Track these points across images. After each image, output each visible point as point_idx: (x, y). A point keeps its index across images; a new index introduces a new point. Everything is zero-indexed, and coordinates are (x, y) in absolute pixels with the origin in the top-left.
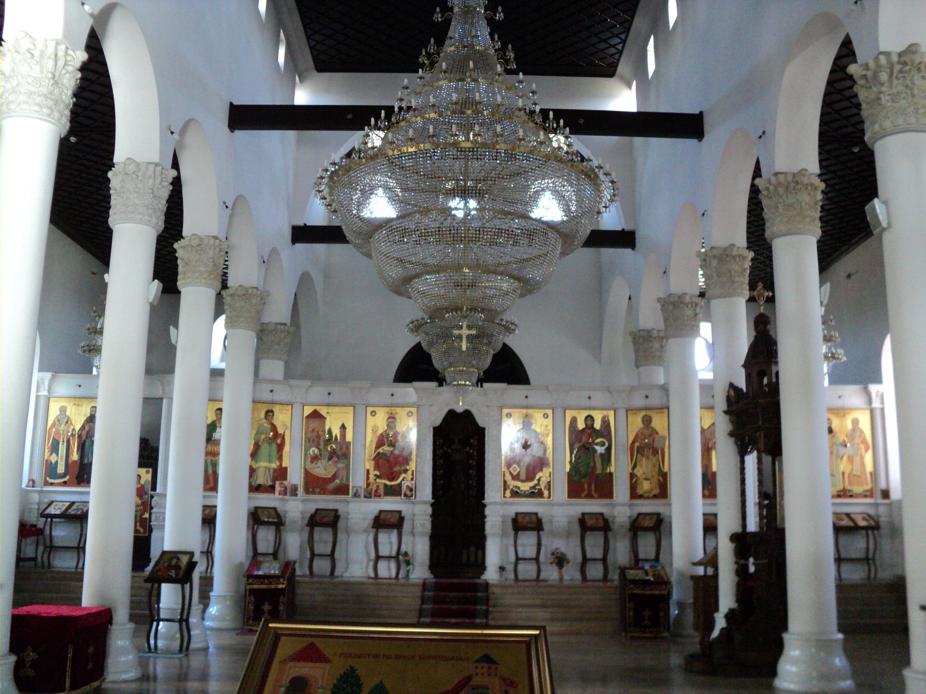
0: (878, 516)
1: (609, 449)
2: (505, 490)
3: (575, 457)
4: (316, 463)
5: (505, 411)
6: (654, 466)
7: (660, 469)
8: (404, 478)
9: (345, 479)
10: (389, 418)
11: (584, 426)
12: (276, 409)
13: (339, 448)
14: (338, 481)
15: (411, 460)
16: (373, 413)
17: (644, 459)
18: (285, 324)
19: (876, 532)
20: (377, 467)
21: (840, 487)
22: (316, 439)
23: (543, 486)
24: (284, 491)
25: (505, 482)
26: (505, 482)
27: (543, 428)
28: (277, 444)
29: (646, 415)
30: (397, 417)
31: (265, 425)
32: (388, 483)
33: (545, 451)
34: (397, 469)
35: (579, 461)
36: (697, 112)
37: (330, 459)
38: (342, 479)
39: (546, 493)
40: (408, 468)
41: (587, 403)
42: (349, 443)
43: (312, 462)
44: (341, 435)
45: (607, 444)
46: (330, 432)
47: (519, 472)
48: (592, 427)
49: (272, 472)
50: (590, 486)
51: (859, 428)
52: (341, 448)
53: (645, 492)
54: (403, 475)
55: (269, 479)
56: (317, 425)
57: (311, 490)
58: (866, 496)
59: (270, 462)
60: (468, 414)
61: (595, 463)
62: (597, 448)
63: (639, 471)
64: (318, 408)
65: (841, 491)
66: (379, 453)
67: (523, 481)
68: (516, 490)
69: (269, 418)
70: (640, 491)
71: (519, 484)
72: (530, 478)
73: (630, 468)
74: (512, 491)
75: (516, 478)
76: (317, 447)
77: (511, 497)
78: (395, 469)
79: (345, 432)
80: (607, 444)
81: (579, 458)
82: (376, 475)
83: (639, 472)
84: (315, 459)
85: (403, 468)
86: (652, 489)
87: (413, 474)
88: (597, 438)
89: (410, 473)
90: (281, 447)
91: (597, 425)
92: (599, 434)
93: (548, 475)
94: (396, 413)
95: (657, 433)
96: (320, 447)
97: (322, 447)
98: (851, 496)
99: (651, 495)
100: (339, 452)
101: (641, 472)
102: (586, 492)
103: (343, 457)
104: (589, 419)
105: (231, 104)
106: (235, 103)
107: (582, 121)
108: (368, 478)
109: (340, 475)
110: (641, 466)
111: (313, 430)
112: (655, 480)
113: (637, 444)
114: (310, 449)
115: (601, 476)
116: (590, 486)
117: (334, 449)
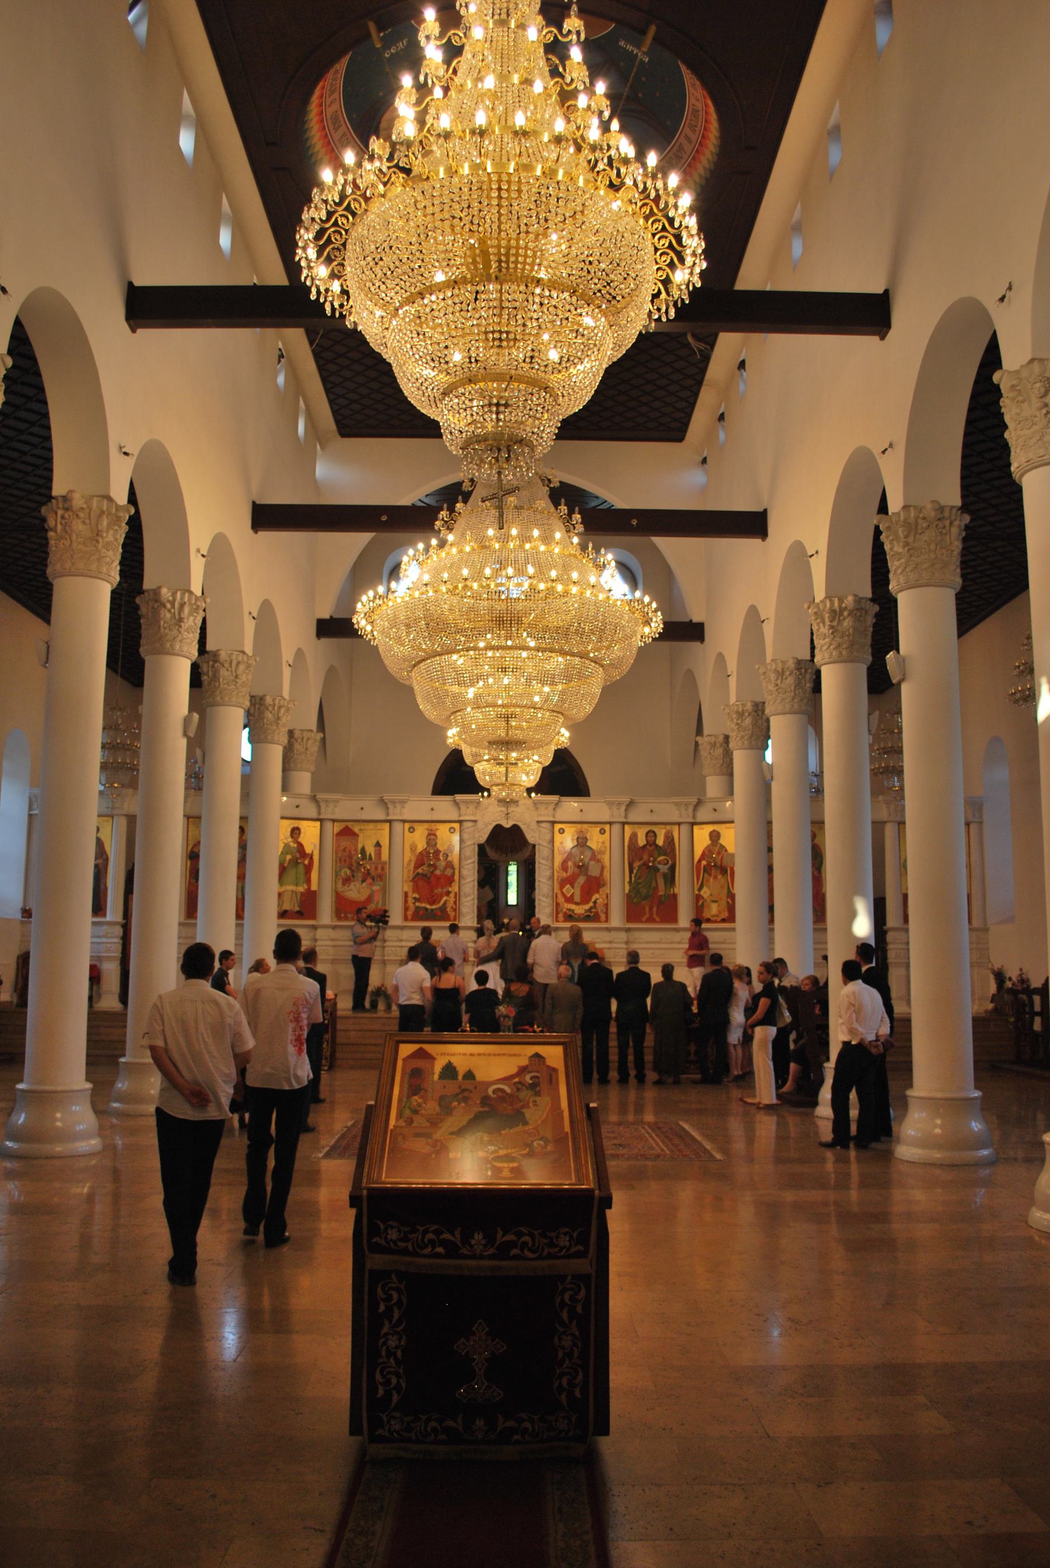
1: (673, 868)
2: (557, 913)
3: (635, 876)
5: (557, 827)
6: (722, 887)
7: (729, 888)
8: (446, 900)
9: (380, 902)
10: (429, 835)
11: (645, 843)
12: (304, 825)
13: (373, 869)
15: (454, 881)
16: (412, 830)
17: (711, 879)
18: (311, 731)
20: (416, 889)
23: (600, 908)
25: (558, 904)
26: (558, 904)
27: (600, 844)
28: (305, 865)
29: (714, 831)
30: (438, 833)
31: (292, 844)
32: (428, 907)
33: (603, 868)
34: (438, 891)
35: (640, 881)
36: (761, 510)
38: (377, 903)
39: (603, 916)
40: (450, 889)
41: (648, 819)
42: (385, 863)
43: (344, 884)
44: (375, 855)
45: (670, 862)
46: (363, 851)
47: (573, 894)
48: (654, 843)
49: (299, 897)
50: (651, 909)
52: (376, 868)
53: (712, 916)
54: (445, 898)
55: (296, 905)
59: (297, 885)
60: (516, 831)
61: (657, 883)
62: (659, 866)
63: (705, 892)
64: (350, 824)
66: (418, 874)
67: (577, 904)
68: (571, 913)
69: (295, 835)
70: (706, 915)
71: (573, 907)
72: (585, 900)
73: (696, 887)
74: (565, 913)
75: (570, 900)
76: (350, 868)
77: (565, 921)
78: (436, 891)
79: (380, 851)
80: (670, 862)
81: (639, 878)
82: (415, 898)
83: (705, 893)
84: (347, 881)
85: (445, 890)
86: (720, 912)
87: (456, 897)
88: (660, 855)
89: (452, 895)
90: (308, 869)
91: (660, 842)
92: (660, 850)
93: (605, 897)
94: (437, 830)
95: (726, 850)
99: (719, 919)
100: (373, 873)
101: (708, 893)
102: (647, 916)
104: (651, 835)
105: (254, 503)
106: (258, 502)
107: (634, 522)
108: (406, 901)
110: (709, 887)
111: (344, 850)
112: (724, 903)
113: (704, 863)
114: (340, 871)
115: (663, 899)
116: (651, 909)
117: (368, 870)
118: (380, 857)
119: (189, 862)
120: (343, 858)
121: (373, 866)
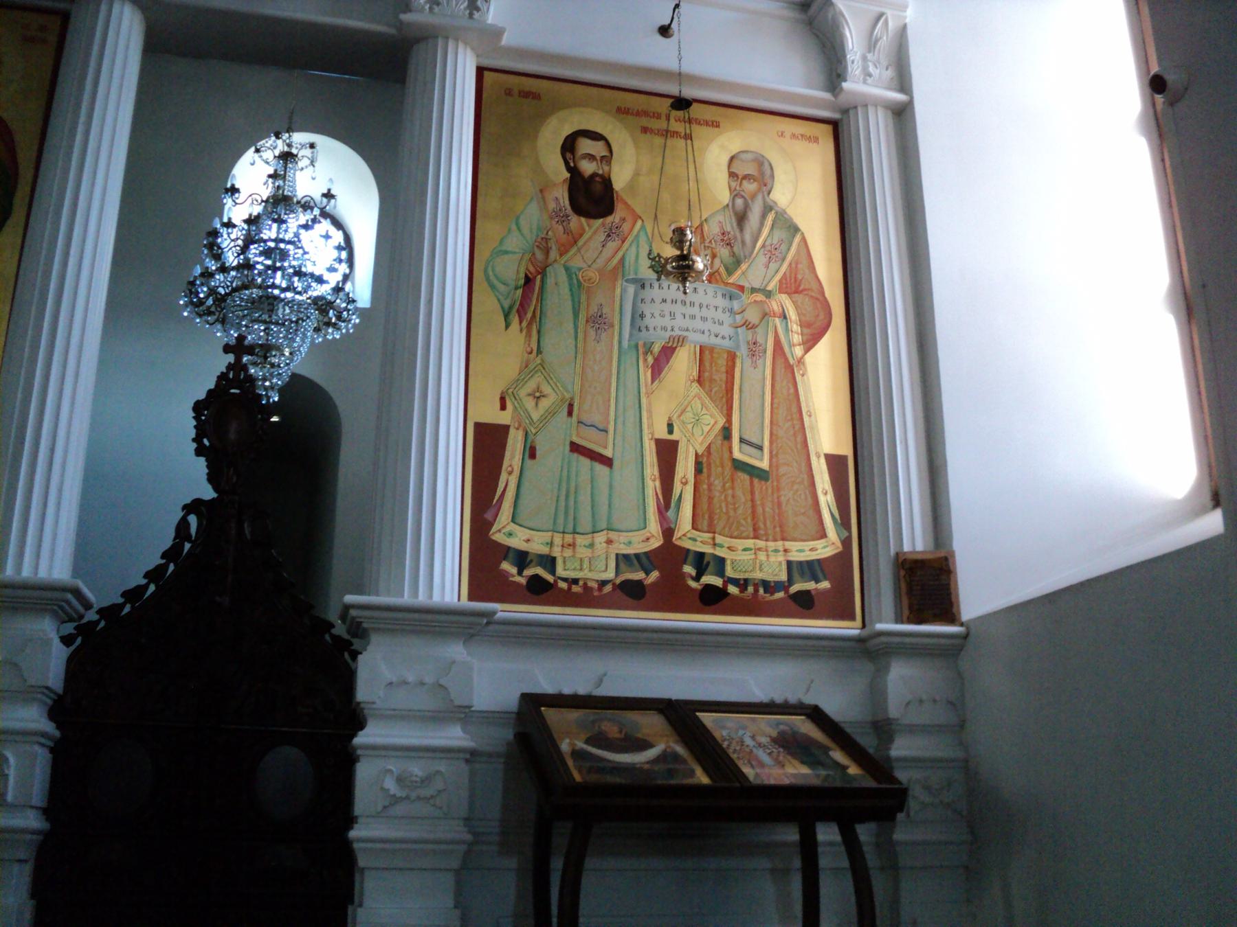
0: (884, 728)
19: (865, 832)
21: (648, 538)
51: (768, 208)
58: (804, 604)
65: (644, 561)
98: (712, 599)
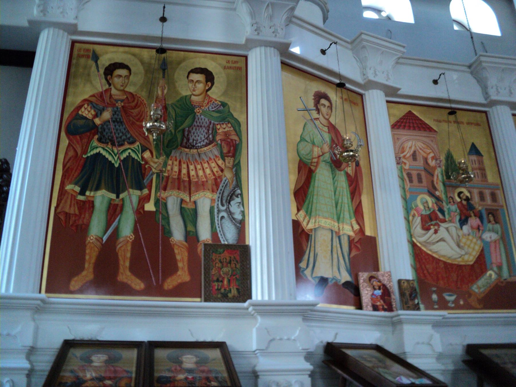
4: (436, 232)
13: (476, 199)
14: (491, 274)
22: (423, 174)
24: (382, 297)
37: (463, 222)
38: (500, 267)
56: (420, 145)
57: (435, 297)
76: (432, 194)
96: (437, 193)
97: (440, 192)
103: (492, 218)
109: (494, 260)
111: (414, 156)
117: (467, 199)
118: (484, 176)
119: (65, 142)
120: (414, 173)
121: (475, 192)
